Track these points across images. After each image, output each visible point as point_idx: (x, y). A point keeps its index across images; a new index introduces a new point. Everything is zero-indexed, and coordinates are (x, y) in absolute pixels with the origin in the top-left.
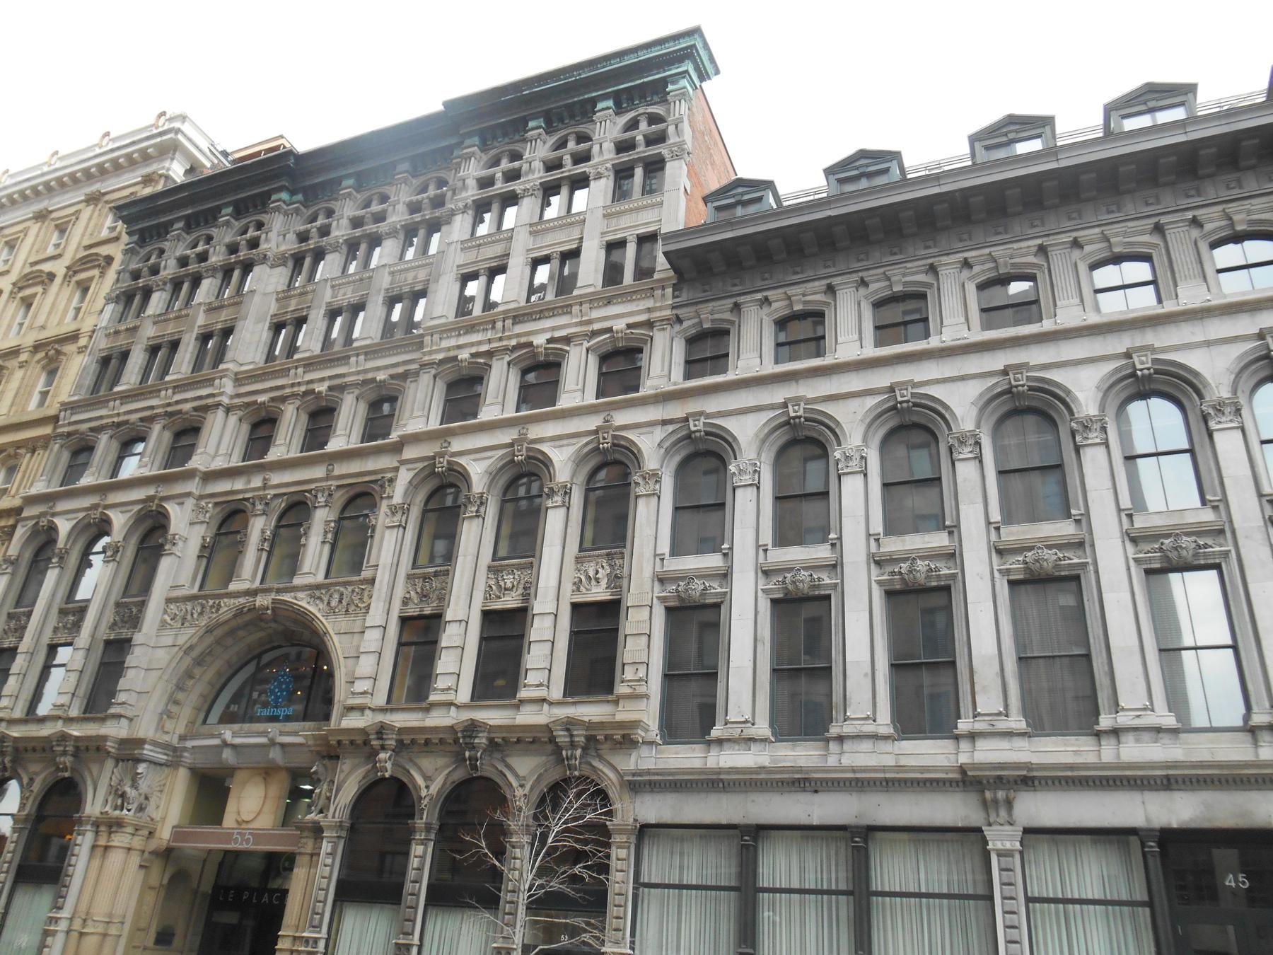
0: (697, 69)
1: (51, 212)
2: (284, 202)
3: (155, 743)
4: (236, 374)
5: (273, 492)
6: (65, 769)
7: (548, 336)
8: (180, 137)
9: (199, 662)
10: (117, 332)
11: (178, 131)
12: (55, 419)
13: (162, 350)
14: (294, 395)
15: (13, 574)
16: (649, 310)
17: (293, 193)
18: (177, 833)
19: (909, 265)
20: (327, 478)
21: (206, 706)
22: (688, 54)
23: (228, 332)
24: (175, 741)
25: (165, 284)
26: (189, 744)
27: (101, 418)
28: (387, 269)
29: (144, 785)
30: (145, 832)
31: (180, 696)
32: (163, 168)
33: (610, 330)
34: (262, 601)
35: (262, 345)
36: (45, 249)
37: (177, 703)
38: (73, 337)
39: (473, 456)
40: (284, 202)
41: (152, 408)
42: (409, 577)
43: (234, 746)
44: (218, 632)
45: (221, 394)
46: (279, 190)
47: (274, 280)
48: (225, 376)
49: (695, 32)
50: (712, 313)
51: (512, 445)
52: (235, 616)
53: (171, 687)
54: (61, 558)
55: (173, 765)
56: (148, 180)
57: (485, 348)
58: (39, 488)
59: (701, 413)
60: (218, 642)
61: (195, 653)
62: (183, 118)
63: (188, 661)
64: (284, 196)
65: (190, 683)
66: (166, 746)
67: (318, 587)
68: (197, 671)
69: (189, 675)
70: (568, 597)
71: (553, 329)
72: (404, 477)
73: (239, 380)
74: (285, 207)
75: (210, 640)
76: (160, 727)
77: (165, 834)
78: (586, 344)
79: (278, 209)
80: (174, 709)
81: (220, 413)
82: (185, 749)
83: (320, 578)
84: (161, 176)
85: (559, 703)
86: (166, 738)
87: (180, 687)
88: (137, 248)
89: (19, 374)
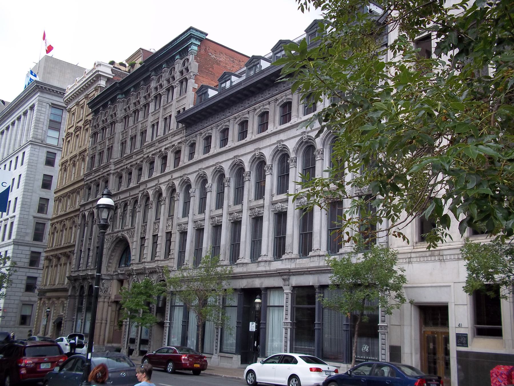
0: (196, 39)
1: (80, 102)
2: (120, 98)
3: (104, 275)
4: (114, 162)
5: (121, 201)
6: (90, 283)
7: (164, 148)
8: (100, 73)
9: (113, 251)
10: (93, 148)
11: (98, 71)
12: (83, 180)
13: (101, 153)
14: (124, 169)
15: (81, 229)
16: (181, 138)
17: (122, 94)
18: (116, 297)
19: (224, 120)
20: (129, 196)
21: (118, 263)
22: (191, 37)
23: (112, 146)
24: (112, 273)
25: (100, 131)
26: (115, 273)
27: (91, 179)
28: (140, 123)
29: (105, 285)
30: (108, 297)
31: (111, 261)
32: (98, 85)
33: (174, 145)
34: (119, 234)
35: (119, 151)
36: (80, 116)
37: (110, 263)
38: (85, 151)
39: (151, 189)
40: (120, 98)
41: (99, 175)
42: (142, 226)
43: (121, 274)
44: (114, 243)
45: (111, 170)
46: (118, 94)
47: (120, 128)
48: (110, 164)
49: (191, 28)
50: (191, 140)
51: (155, 186)
52: (116, 239)
53: (108, 259)
54: (87, 224)
55: (112, 279)
56: (96, 90)
57: (154, 152)
58: (83, 202)
59: (185, 174)
60: (115, 246)
61: (111, 250)
62: (100, 65)
63: (110, 252)
64: (120, 96)
65: (112, 257)
66: (108, 275)
67: (128, 230)
68: (113, 254)
69: (111, 255)
70: (165, 231)
71: (165, 145)
72: (140, 195)
73: (116, 164)
74: (121, 100)
75: (113, 246)
76: (107, 270)
77: (113, 297)
78: (171, 150)
79: (119, 102)
80: (110, 265)
81: (111, 176)
82: (114, 275)
83: (130, 227)
84: (99, 87)
85: (163, 260)
86: (109, 273)
87: (110, 259)
88: (95, 117)
89: (78, 163)
